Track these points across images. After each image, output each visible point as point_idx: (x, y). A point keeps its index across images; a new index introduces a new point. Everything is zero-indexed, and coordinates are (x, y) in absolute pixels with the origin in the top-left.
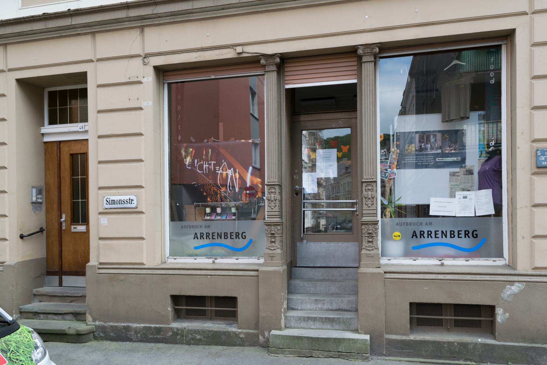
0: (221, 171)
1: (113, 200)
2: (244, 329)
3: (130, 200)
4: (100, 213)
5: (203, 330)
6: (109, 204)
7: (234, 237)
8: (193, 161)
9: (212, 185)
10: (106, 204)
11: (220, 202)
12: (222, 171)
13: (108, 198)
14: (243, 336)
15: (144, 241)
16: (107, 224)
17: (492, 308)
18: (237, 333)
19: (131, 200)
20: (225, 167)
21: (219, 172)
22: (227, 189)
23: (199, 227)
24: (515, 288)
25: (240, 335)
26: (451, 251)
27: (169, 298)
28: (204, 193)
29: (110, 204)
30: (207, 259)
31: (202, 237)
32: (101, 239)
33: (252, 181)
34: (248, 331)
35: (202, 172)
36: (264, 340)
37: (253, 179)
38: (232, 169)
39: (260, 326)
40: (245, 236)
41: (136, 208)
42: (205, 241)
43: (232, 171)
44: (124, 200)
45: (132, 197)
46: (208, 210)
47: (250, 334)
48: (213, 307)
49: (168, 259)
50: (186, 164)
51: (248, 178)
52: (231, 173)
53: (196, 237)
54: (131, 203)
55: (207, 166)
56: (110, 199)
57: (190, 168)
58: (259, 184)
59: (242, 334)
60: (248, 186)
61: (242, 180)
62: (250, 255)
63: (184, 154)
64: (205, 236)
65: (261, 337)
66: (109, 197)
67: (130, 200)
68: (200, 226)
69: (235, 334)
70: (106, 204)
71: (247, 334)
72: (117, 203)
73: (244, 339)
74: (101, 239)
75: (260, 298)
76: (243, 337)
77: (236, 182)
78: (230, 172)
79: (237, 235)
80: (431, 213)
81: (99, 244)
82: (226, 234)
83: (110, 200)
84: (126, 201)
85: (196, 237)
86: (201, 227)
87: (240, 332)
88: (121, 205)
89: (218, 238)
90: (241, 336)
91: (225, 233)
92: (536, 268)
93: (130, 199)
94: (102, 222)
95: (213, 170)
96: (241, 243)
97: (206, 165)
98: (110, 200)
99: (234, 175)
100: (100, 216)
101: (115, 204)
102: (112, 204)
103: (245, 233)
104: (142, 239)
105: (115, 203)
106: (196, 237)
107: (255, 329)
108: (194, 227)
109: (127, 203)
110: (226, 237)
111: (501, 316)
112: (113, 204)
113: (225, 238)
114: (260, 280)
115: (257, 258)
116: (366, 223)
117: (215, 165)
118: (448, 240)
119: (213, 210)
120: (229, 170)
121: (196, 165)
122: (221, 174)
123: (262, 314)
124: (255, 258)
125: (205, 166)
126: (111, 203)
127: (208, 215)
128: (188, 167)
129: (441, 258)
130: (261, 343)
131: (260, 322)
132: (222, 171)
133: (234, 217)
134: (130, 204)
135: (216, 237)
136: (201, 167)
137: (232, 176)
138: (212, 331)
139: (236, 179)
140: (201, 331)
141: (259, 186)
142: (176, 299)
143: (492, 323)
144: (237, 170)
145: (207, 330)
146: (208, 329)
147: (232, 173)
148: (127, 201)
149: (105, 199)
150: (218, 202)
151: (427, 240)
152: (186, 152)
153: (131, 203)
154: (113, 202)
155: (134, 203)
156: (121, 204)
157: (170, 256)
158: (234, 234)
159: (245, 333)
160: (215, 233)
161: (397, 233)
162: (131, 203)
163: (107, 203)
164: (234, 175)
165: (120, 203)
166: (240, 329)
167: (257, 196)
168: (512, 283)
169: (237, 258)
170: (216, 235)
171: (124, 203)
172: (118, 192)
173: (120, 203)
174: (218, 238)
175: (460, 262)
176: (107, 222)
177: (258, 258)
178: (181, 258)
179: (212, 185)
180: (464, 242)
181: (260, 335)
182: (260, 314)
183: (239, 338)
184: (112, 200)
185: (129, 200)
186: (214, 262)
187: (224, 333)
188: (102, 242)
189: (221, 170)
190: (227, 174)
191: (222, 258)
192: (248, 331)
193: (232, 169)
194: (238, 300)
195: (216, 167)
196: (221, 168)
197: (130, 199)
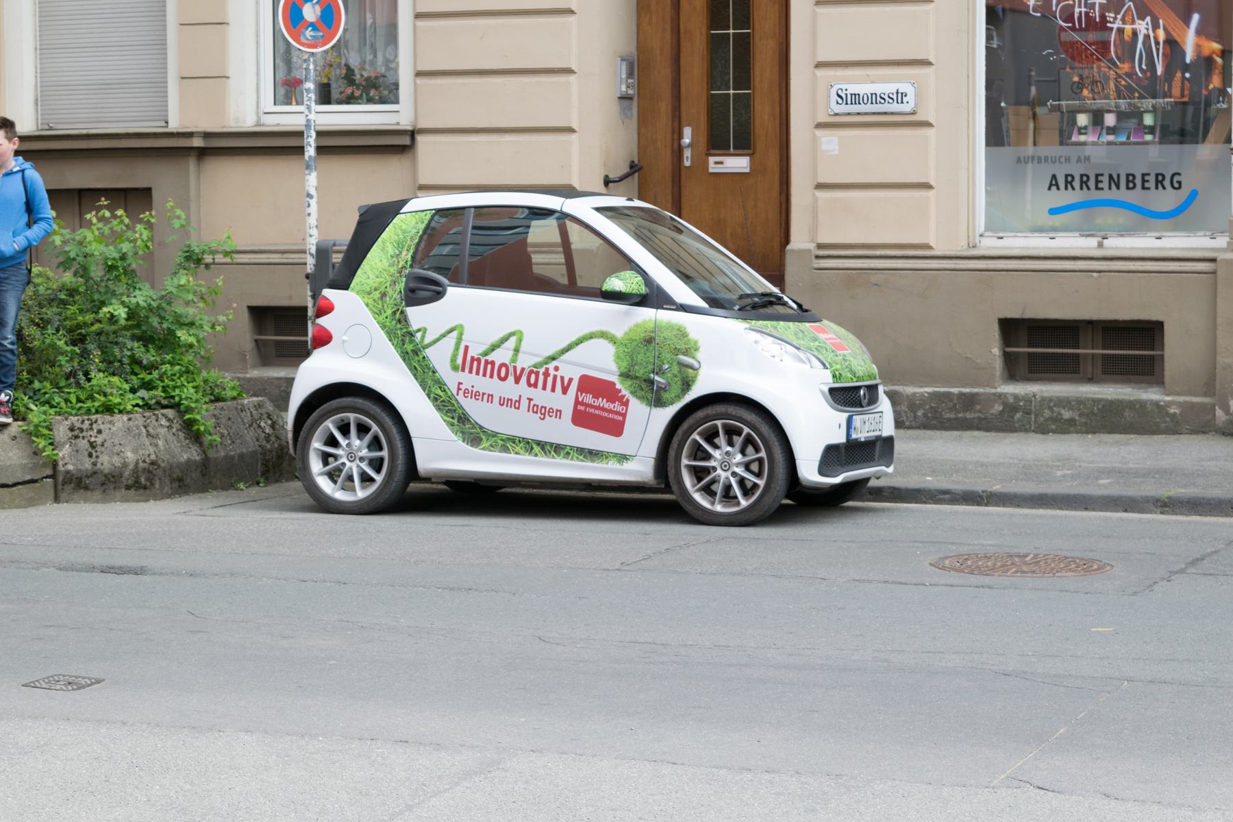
0: (1120, 22)
1: (855, 95)
2: (1178, 394)
3: (900, 95)
4: (820, 126)
5: (1080, 397)
6: (845, 102)
7: (1152, 184)
9: (1095, 57)
10: (837, 103)
11: (1115, 99)
12: (1123, 23)
13: (842, 90)
14: (1176, 411)
15: (931, 193)
16: (836, 152)
18: (1162, 403)
19: (902, 94)
20: (1130, 13)
21: (1115, 26)
22: (1134, 67)
23: (1063, 160)
25: (1168, 409)
27: (996, 327)
28: (1072, 78)
29: (847, 104)
30: (1083, 239)
31: (1069, 182)
32: (820, 186)
33: (1198, 47)
34: (1188, 399)
35: (1070, 25)
36: (1227, 419)
37: (1200, 43)
38: (1148, 19)
39: (1218, 387)
40: (1180, 183)
41: (914, 113)
42: (1074, 196)
43: (1147, 24)
44: (884, 94)
45: (903, 87)
46: (1082, 120)
47: (1192, 405)
48: (1097, 349)
49: (981, 239)
50: (1029, 6)
51: (1190, 43)
52: (1146, 28)
53: (1054, 183)
54: (900, 101)
55: (1083, 10)
56: (846, 92)
57: (1039, 15)
58: (1218, 56)
59: (1173, 407)
60: (1188, 61)
61: (1173, 45)
62: (1190, 228)
64: (1077, 184)
65: (1219, 413)
66: (844, 87)
67: (900, 95)
68: (1066, 157)
69: (1159, 405)
70: (837, 103)
71: (1184, 406)
72: (865, 102)
73: (1179, 418)
74: (820, 186)
75: (1219, 321)
76: (1176, 413)
77: (1158, 50)
78: (1143, 26)
79: (1159, 182)
81: (816, 199)
82: (1131, 178)
83: (846, 94)
84: (884, 99)
85: (1054, 185)
86: (1068, 160)
87: (1169, 402)
88: (875, 105)
89: (1110, 188)
90: (1172, 411)
91: (1128, 175)
93: (897, 93)
94: (824, 147)
95: (1098, 20)
96: (1166, 199)
97: (1080, 6)
98: (846, 94)
99: (1152, 35)
100: (819, 132)
101: (859, 103)
102: (852, 104)
103: (1179, 174)
104: (927, 186)
105: (861, 102)
106: (1054, 183)
107: (1205, 395)
108: (1049, 161)
109: (891, 101)
110: (1131, 185)
112: (856, 104)
113: (1128, 188)
114: (1219, 281)
115: (1209, 236)
119: (1097, 118)
120: (1140, 22)
121: (1054, 9)
122: (1121, 31)
123: (1221, 360)
124: (1205, 236)
125: (1077, 10)
126: (849, 102)
127: (1083, 131)
128: (1033, 11)
130: (1220, 425)
131: (1218, 380)
132: (1123, 23)
133: (1149, 137)
134: (898, 103)
135: (1105, 184)
137: (1147, 37)
138: (1099, 400)
139: (1157, 43)
140: (1074, 401)
141: (1216, 61)
142: (1010, 329)
144: (1161, 21)
145: (1088, 399)
146: (1091, 396)
147: (1147, 29)
148: (891, 95)
149: (833, 92)
150: (1109, 99)
153: (902, 102)
154: (856, 98)
155: (908, 102)
156: (876, 103)
157: (986, 230)
158: (1152, 179)
159: (1180, 405)
160: (1102, 175)
162: (900, 101)
163: (840, 101)
164: (1152, 35)
165: (874, 102)
166: (1168, 395)
167: (1211, 86)
169: (1158, 235)
170: (1105, 179)
171: (882, 101)
172: (868, 75)
173: (874, 102)
174: (1110, 188)
176: (837, 148)
177: (1213, 234)
178: (1016, 236)
179: (1095, 57)
181: (1217, 408)
182: (1219, 359)
183: (1168, 414)
184: (852, 95)
185: (895, 95)
186: (1100, 245)
187: (1131, 405)
188: (822, 195)
189: (1121, 20)
190: (1135, 33)
191: (1122, 236)
192: (1188, 399)
193: (1148, 19)
194: (1166, 327)
195: (1107, 14)
196: (1119, 17)
197: (899, 91)
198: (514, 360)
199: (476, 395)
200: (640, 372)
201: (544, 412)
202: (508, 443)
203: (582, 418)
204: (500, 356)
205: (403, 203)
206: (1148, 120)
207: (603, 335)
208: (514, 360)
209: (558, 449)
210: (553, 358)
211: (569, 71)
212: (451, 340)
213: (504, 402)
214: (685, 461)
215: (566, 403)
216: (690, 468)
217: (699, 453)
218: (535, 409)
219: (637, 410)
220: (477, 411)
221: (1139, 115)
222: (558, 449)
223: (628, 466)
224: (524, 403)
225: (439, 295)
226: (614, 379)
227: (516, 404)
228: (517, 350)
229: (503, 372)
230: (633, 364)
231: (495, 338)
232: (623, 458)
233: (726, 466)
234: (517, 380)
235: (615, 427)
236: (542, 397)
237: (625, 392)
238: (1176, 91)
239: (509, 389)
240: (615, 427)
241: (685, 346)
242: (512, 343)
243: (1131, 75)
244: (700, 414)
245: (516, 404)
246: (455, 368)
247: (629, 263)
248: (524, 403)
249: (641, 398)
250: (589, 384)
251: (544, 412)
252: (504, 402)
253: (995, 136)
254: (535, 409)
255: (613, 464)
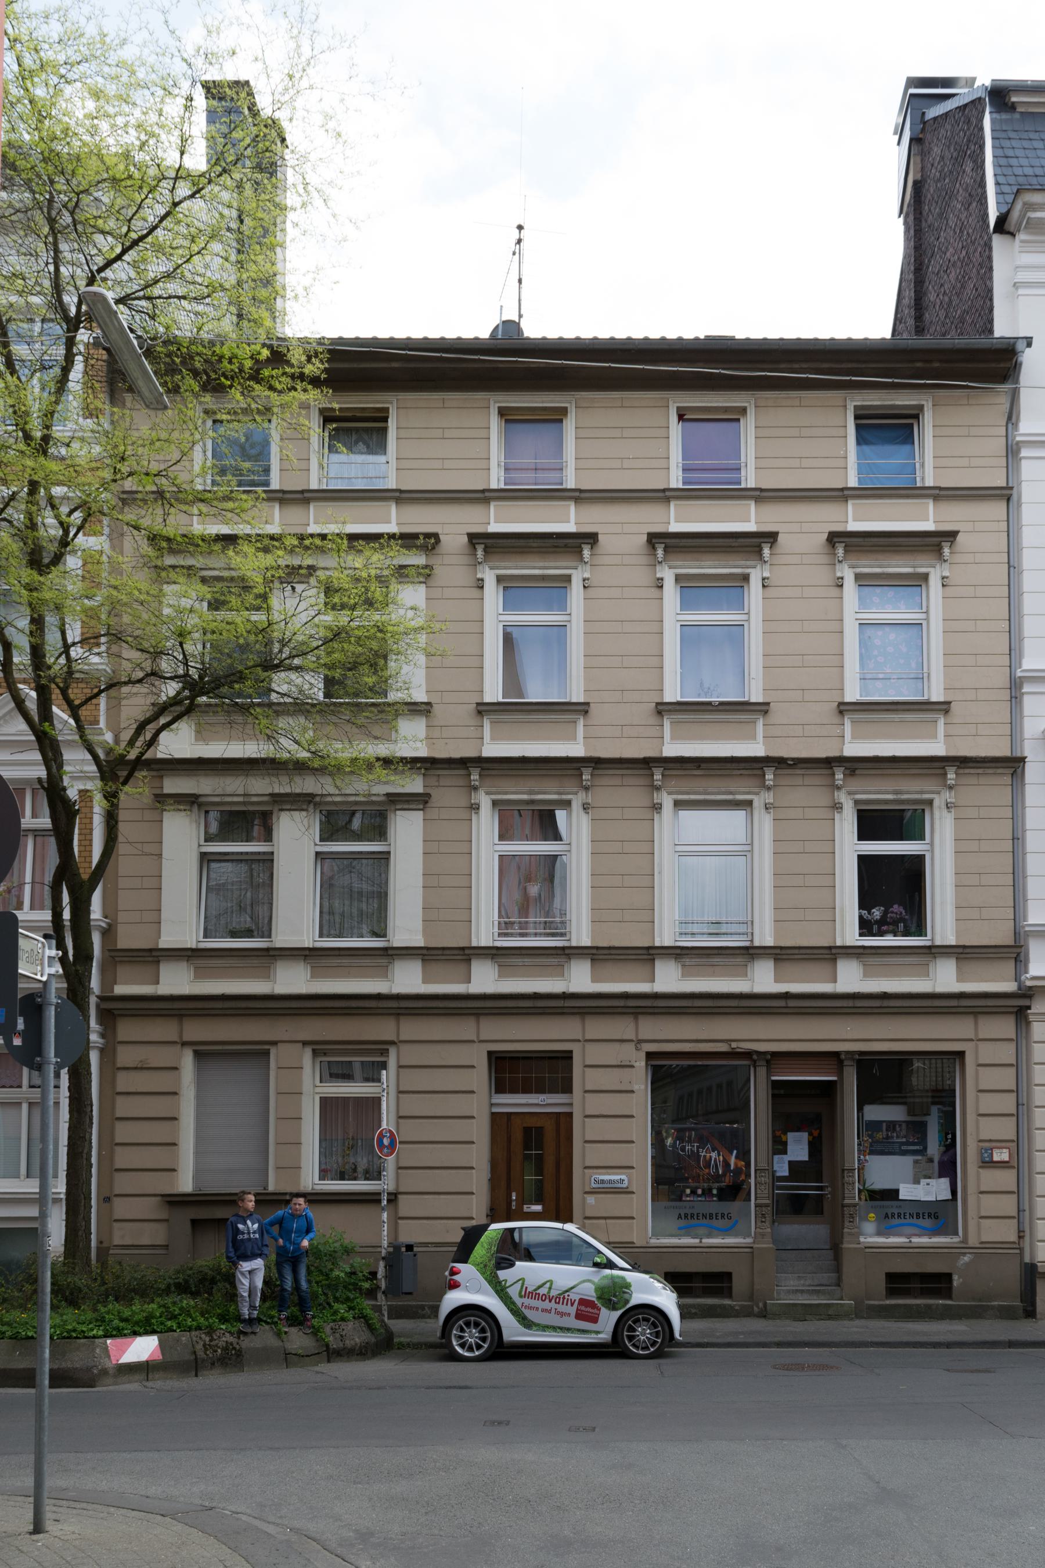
8: (675, 1143)
17: (948, 1277)
24: (966, 1259)
26: (916, 1231)
51: (733, 1161)
61: (727, 1164)
63: (664, 1134)
78: (714, 1155)
80: (901, 1197)
92: (982, 1243)
111: (956, 1281)
116: (849, 1206)
117: (698, 1147)
118: (915, 1221)
129: (909, 1236)
136: (683, 1149)
143: (950, 1288)
151: (896, 1221)
152: (667, 1132)
161: (872, 1215)
168: (964, 1254)
175: (924, 1240)
180: (927, 1223)
198: (549, 1292)
199: (530, 1308)
200: (606, 1297)
201: (562, 1314)
202: (545, 1328)
203: (579, 1316)
204: (542, 1291)
205: (488, 1226)
206: (715, 1192)
207: (589, 1281)
208: (549, 1292)
209: (568, 1330)
210: (567, 1291)
211: (472, 1168)
212: (519, 1285)
213: (544, 1310)
214: (626, 1333)
215: (573, 1310)
216: (628, 1336)
217: (632, 1329)
218: (558, 1313)
219: (604, 1312)
220: (530, 1314)
221: (710, 1190)
222: (568, 1330)
223: (600, 1336)
224: (553, 1311)
225: (512, 1265)
226: (594, 1299)
227: (549, 1311)
228: (550, 1288)
229: (544, 1298)
230: (603, 1293)
231: (540, 1283)
232: (597, 1332)
233: (643, 1334)
234: (550, 1301)
235: (594, 1320)
236: (561, 1308)
237: (599, 1305)
238: (727, 1180)
239: (546, 1305)
240: (594, 1320)
241: (624, 1287)
242: (548, 1285)
243: (709, 1174)
244: (632, 1313)
245: (549, 1311)
246: (521, 1296)
247: (599, 1252)
248: (553, 1311)
249: (606, 1307)
250: (582, 1302)
251: (562, 1314)
252: (544, 1310)
253: (654, 1199)
254: (558, 1313)
255: (593, 1335)
